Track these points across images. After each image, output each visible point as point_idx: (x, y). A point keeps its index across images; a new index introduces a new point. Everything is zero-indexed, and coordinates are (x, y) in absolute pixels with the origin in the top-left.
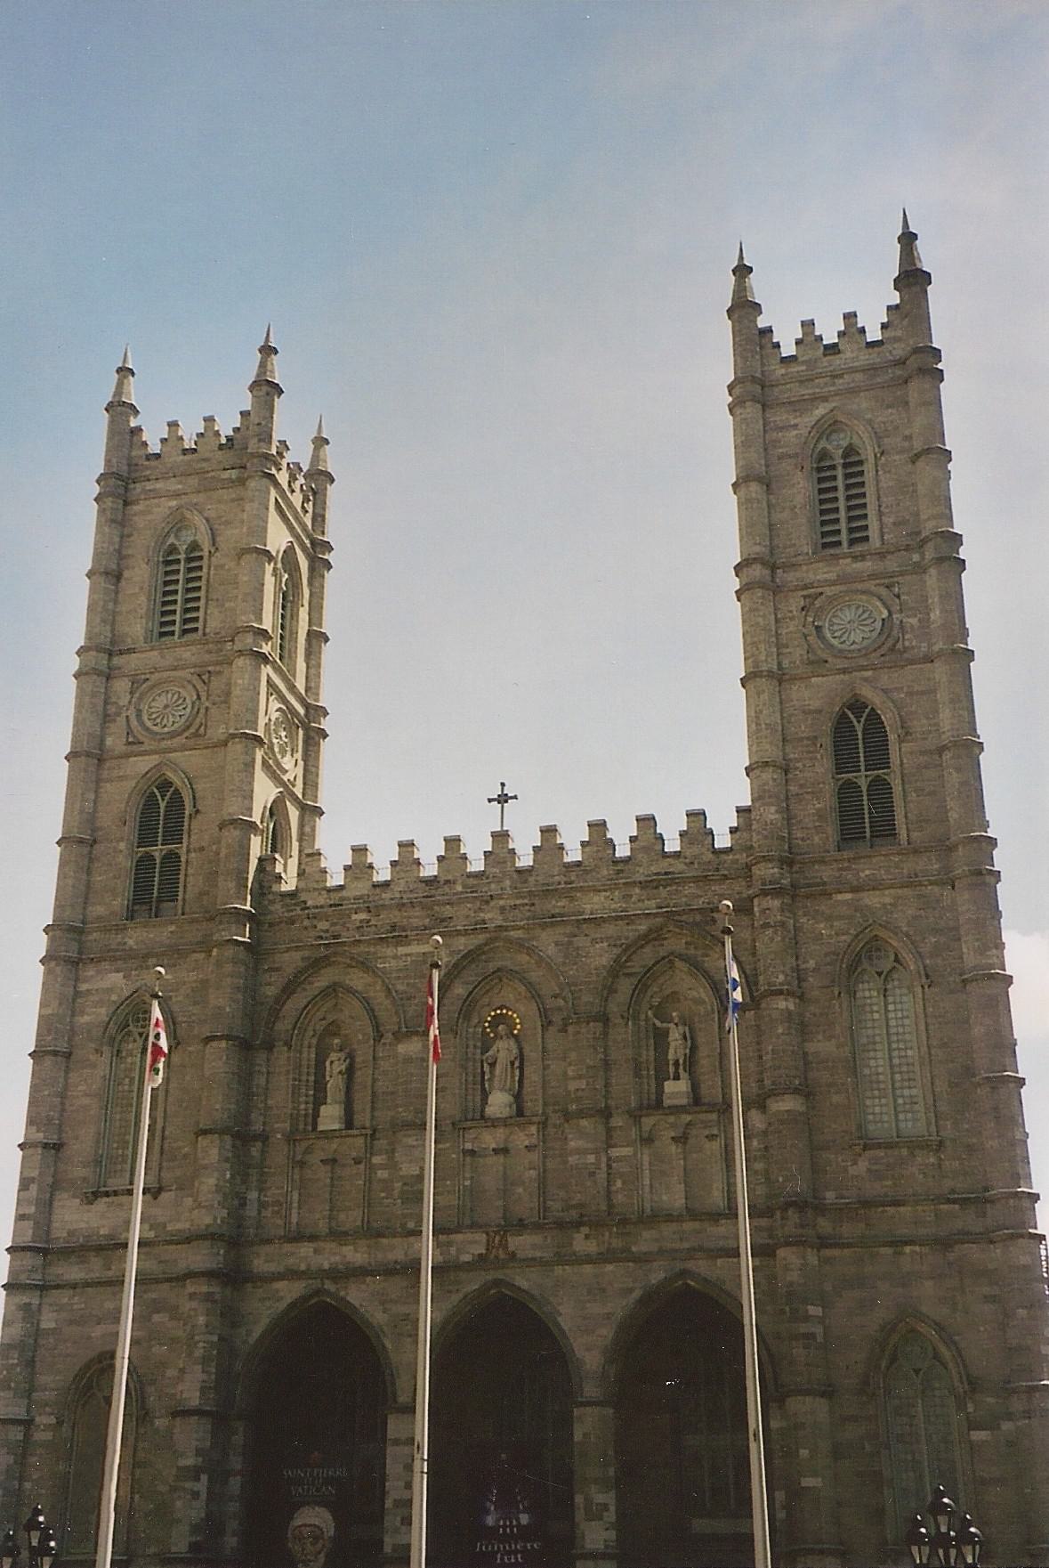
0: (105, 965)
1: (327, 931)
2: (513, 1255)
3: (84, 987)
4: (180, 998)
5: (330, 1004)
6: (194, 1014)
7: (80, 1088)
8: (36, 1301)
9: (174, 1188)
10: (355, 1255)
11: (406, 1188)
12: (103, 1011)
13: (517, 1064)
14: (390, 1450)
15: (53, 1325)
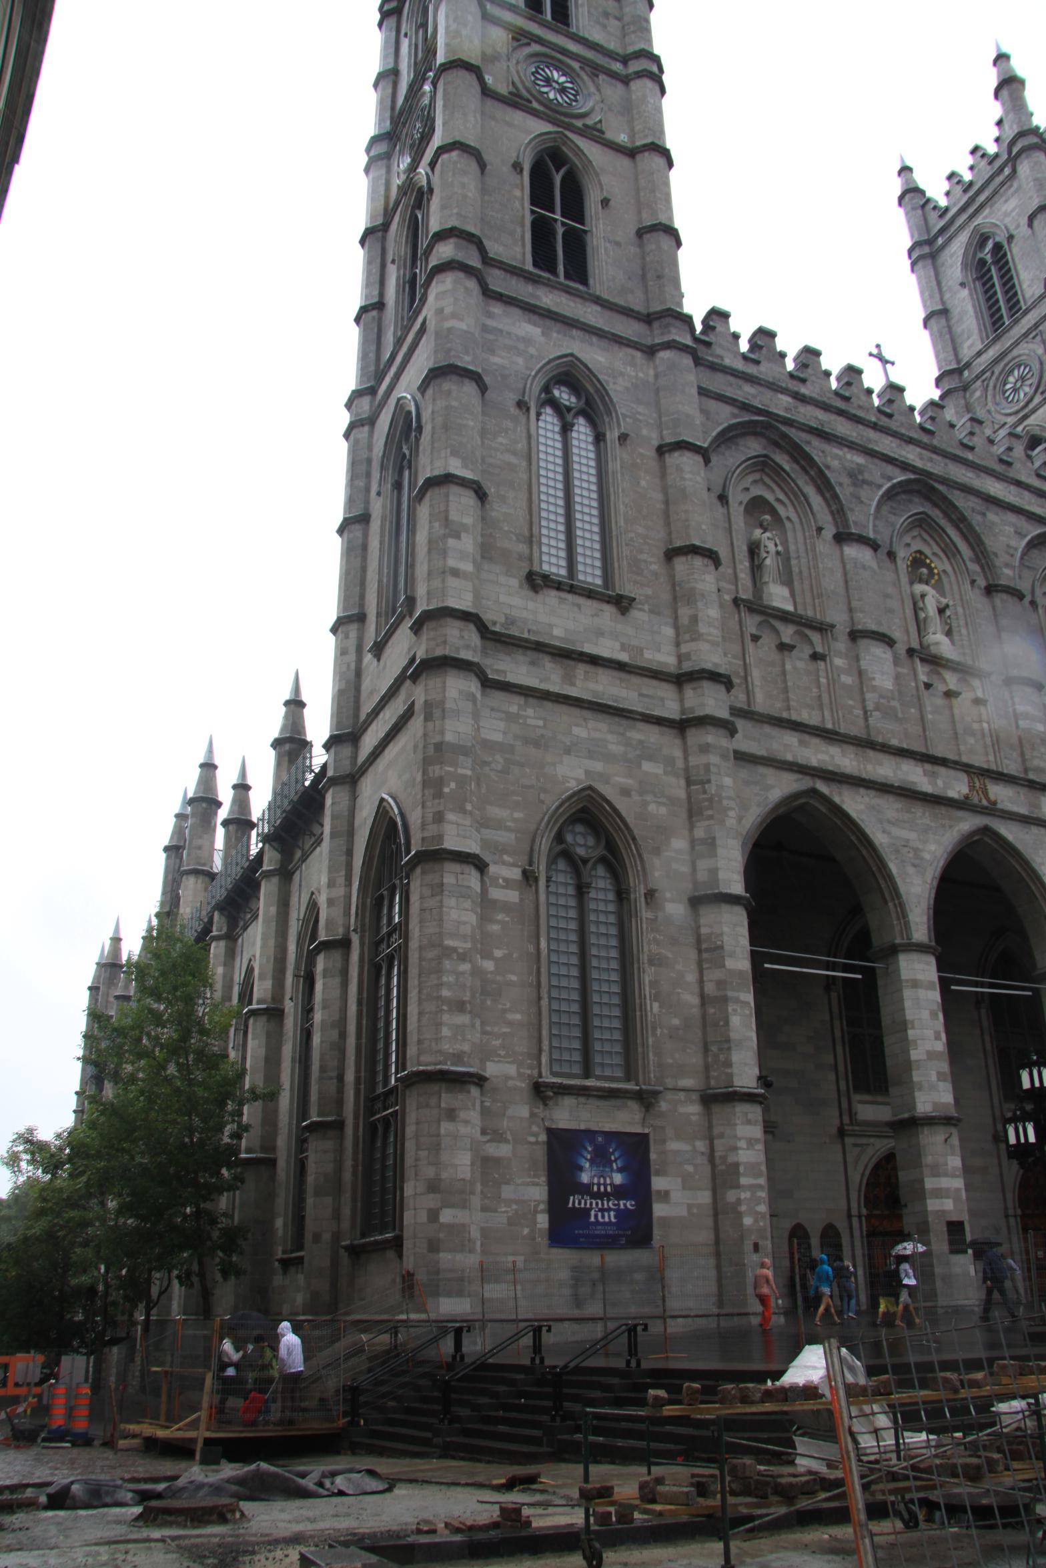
0: (516, 311)
1: (754, 396)
2: (995, 803)
3: (491, 323)
4: (619, 388)
5: (757, 476)
6: (639, 413)
7: (504, 441)
8: (479, 695)
9: (646, 607)
10: (844, 760)
11: (882, 701)
12: (520, 360)
13: (948, 613)
14: (907, 993)
15: (497, 737)
